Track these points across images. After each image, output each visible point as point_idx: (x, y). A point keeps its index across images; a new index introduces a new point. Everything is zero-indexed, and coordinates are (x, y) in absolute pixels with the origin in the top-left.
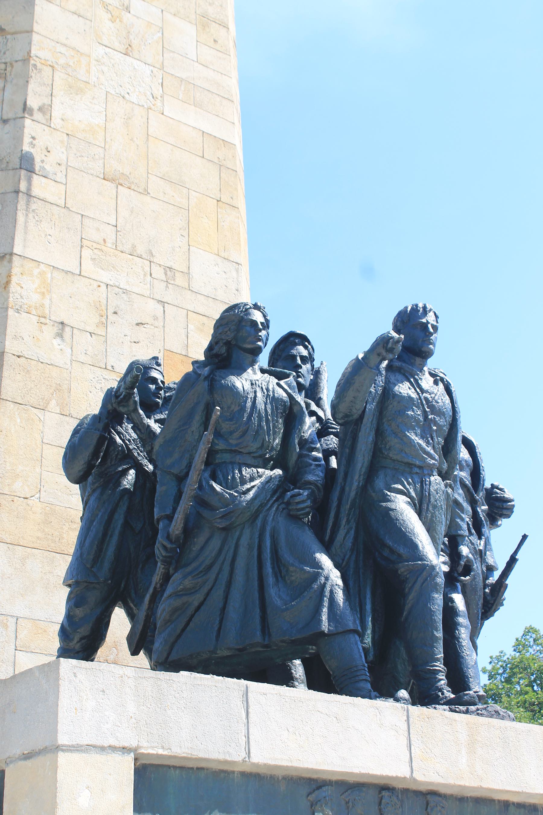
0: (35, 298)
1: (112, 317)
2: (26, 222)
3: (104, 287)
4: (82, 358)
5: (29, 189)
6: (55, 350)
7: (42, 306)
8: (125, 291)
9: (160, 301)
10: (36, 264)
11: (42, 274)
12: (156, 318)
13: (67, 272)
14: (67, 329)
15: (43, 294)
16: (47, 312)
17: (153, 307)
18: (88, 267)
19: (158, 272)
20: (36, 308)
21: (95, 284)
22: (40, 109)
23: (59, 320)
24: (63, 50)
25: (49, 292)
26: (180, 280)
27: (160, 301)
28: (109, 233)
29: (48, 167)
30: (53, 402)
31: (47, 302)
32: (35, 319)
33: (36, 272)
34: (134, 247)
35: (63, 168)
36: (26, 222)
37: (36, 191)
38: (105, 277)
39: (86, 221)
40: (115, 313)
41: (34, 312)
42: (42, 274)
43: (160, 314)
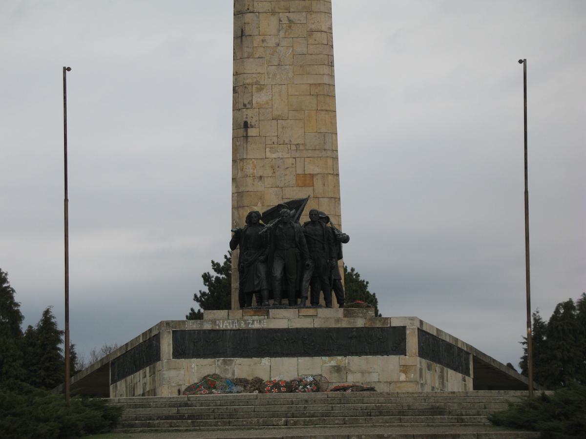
0: (251, 171)
1: (278, 169)
2: (247, 146)
3: (274, 159)
4: (268, 186)
5: (247, 134)
6: (259, 187)
7: (254, 173)
8: (282, 158)
9: (294, 158)
10: (250, 160)
11: (253, 162)
12: (293, 164)
13: (261, 159)
14: (263, 178)
15: (254, 169)
16: (256, 174)
17: (291, 161)
18: (268, 155)
19: (293, 147)
20: (252, 174)
21: (271, 159)
22: (249, 103)
23: (258, 176)
24: (254, 75)
25: (256, 167)
26: (301, 147)
27: (294, 158)
28: (275, 139)
29: (253, 124)
31: (255, 171)
32: (252, 178)
33: (251, 162)
34: (284, 141)
35: (258, 122)
36: (247, 146)
37: (249, 134)
38: (274, 156)
39: (267, 138)
40: (278, 167)
41: (251, 176)
42: (253, 162)
43: (294, 162)
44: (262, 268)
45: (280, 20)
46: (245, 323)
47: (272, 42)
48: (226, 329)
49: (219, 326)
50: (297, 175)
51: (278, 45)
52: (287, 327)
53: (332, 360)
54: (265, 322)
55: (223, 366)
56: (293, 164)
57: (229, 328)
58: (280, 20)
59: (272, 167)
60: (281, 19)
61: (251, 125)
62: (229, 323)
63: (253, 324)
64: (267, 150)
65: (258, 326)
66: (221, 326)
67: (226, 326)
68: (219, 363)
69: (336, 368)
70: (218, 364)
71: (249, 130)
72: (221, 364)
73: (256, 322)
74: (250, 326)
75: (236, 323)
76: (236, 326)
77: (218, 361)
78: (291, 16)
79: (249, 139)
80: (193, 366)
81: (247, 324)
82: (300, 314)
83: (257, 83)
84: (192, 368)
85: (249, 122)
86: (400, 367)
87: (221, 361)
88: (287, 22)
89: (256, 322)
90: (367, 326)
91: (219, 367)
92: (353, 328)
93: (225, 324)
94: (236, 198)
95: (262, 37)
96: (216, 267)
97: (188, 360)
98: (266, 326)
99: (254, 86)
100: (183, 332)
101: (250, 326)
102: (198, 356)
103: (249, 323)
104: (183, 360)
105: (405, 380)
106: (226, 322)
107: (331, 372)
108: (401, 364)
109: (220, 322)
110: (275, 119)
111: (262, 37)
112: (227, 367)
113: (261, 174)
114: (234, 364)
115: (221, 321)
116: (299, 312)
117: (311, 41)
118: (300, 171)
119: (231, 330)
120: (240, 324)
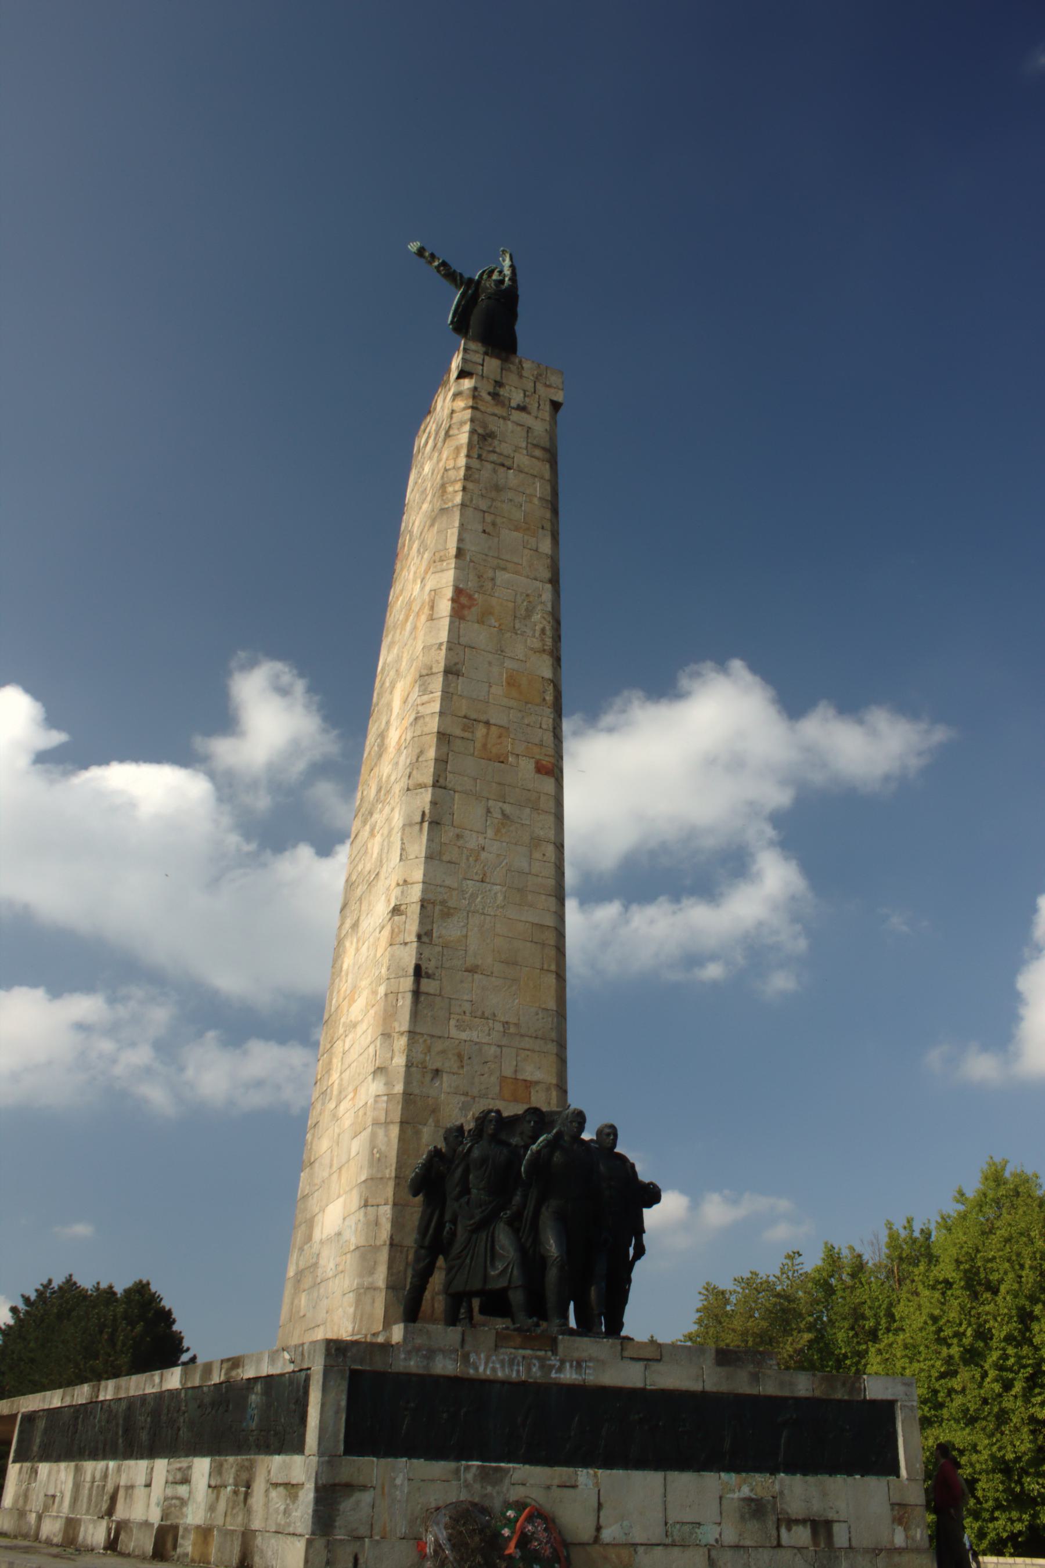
7: (425, 1061)
8: (476, 1043)
11: (425, 1041)
17: (493, 1050)
18: (454, 1032)
19: (499, 1027)
23: (435, 1068)
26: (512, 1030)
28: (467, 1007)
29: (430, 972)
30: (431, 1120)
31: (428, 1058)
33: (421, 1041)
34: (483, 1013)
38: (464, 1036)
43: (498, 1053)
44: (504, 1240)
45: (488, 811)
46: (542, 1367)
47: (473, 841)
48: (492, 1378)
49: (476, 1369)
50: (503, 1079)
51: (483, 849)
52: (640, 1385)
53: (745, 1481)
54: (589, 1367)
55: (477, 1486)
56: (496, 1057)
57: (500, 1374)
58: (488, 811)
59: (460, 1056)
60: (492, 810)
61: (426, 973)
62: (502, 1362)
63: (560, 1370)
64: (452, 1022)
65: (574, 1376)
66: (481, 1369)
67: (494, 1369)
68: (470, 1476)
69: (753, 1504)
70: (465, 1481)
71: (424, 981)
72: (475, 1481)
73: (568, 1365)
74: (553, 1375)
75: (518, 1365)
76: (518, 1371)
77: (467, 1468)
78: (508, 808)
79: (422, 998)
80: (398, 1482)
81: (546, 1368)
82: (626, 1354)
83: (443, 903)
84: (395, 1486)
85: (423, 968)
86: (892, 1509)
87: (474, 1470)
88: (500, 816)
89: (568, 1365)
90: (818, 1394)
91: (467, 1485)
92: (785, 1399)
93: (491, 1365)
94: (384, 1105)
95: (457, 831)
96: (27, 1300)
97: (383, 1461)
98: (591, 1378)
99: (438, 908)
100: (381, 1377)
101: (553, 1375)
102: (411, 1453)
103: (551, 1367)
104: (375, 1459)
105: (903, 1545)
106: (494, 1358)
107: (742, 1518)
108: (893, 1500)
109: (480, 1359)
110: (472, 970)
111: (457, 831)
112: (489, 1489)
113: (438, 1065)
114: (507, 1481)
115: (482, 1356)
116: (622, 1349)
117: (537, 855)
118: (508, 1072)
119: (503, 1383)
120: (529, 1369)
